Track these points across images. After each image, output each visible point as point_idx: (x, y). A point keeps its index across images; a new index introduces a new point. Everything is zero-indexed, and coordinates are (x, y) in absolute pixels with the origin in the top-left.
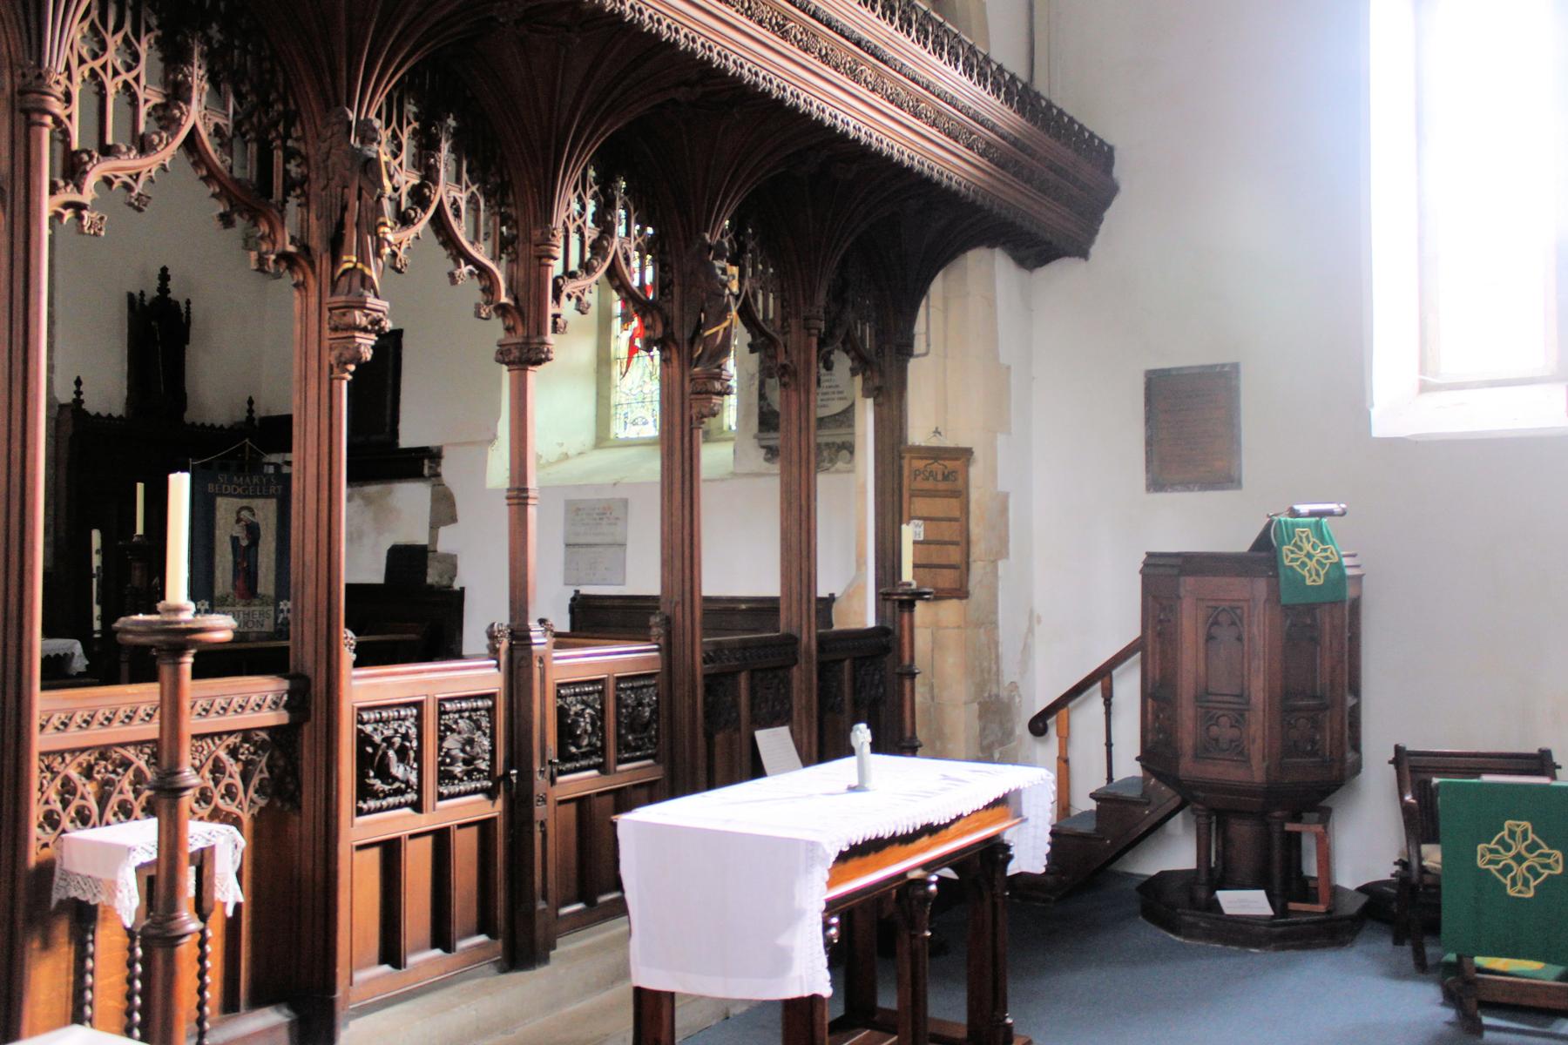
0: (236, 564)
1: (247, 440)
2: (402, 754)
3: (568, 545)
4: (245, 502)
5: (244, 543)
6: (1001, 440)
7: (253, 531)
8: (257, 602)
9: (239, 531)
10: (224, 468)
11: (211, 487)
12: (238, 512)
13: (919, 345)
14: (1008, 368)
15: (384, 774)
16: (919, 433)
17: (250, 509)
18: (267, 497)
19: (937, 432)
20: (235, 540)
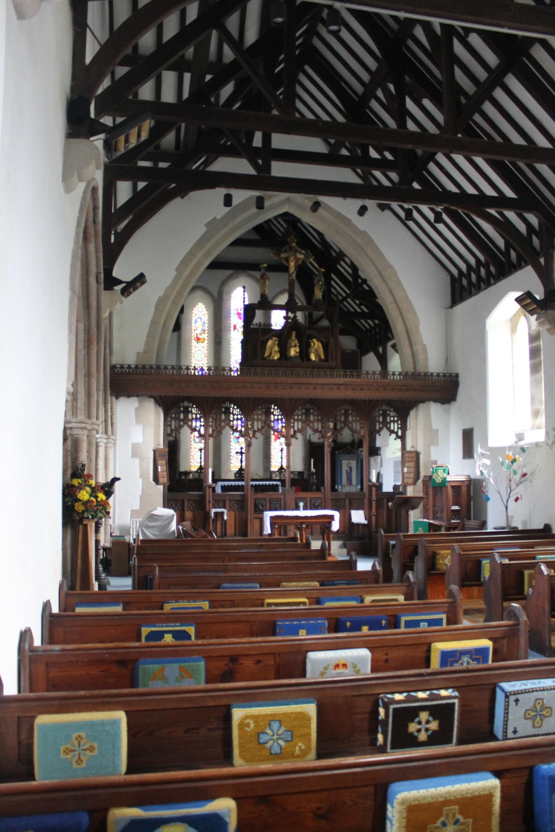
0: (347, 477)
1: (349, 446)
2: (262, 506)
3: (395, 472)
4: (348, 461)
5: (349, 471)
6: (433, 448)
7: (351, 469)
8: (352, 486)
9: (348, 469)
10: (344, 453)
11: (341, 458)
12: (347, 464)
13: (408, 427)
14: (437, 430)
15: (258, 508)
16: (409, 448)
17: (350, 463)
18: (353, 460)
19: (412, 447)
20: (347, 471)
